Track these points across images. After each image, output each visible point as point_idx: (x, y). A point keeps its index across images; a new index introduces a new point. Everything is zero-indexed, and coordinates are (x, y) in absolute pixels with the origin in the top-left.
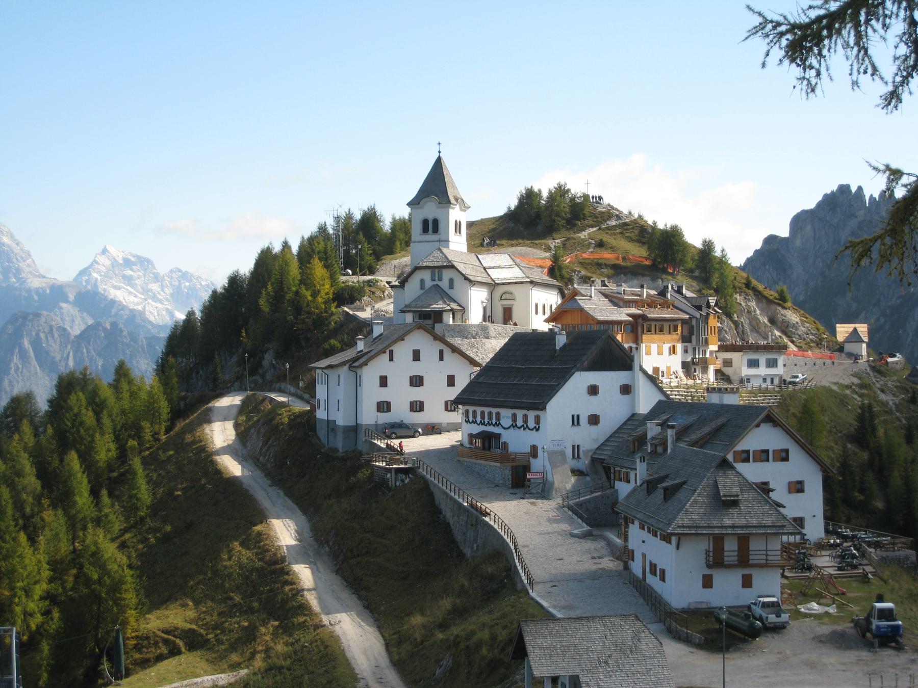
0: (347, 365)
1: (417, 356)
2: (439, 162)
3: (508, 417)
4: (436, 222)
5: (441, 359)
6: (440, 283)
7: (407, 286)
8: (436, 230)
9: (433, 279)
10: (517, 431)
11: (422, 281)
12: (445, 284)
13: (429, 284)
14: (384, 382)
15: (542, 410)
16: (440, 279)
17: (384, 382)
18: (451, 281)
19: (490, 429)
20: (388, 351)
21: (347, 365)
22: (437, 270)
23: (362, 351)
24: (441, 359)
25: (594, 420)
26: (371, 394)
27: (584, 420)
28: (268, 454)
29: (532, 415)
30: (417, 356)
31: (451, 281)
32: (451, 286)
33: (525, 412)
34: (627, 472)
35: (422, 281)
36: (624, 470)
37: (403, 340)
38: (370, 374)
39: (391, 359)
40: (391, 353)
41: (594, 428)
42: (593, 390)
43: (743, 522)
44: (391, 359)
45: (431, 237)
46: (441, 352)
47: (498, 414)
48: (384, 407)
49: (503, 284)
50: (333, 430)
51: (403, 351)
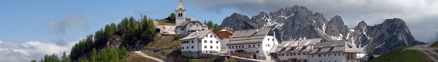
4: (182, 14)
8: (182, 16)
10: (250, 48)
11: (191, 25)
17: (206, 42)
19: (239, 49)
22: (194, 22)
27: (267, 45)
28: (171, 59)
31: (197, 25)
32: (197, 26)
33: (254, 44)
35: (191, 25)
43: (354, 50)
45: (180, 17)
48: (206, 47)
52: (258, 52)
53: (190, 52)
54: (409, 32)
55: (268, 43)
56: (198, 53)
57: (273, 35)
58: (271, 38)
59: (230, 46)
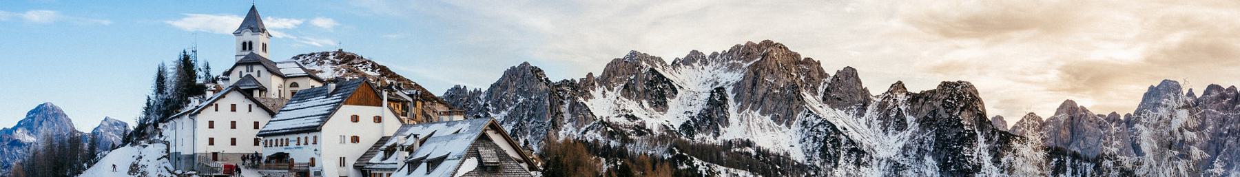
0: (188, 115)
1: (233, 108)
2: (253, 8)
3: (294, 141)
4: (251, 43)
5: (250, 111)
6: (251, 74)
7: (230, 77)
9: (247, 71)
11: (241, 72)
12: (254, 74)
13: (244, 74)
14: (211, 125)
15: (318, 131)
16: (252, 71)
17: (211, 125)
18: (259, 72)
20: (214, 104)
21: (188, 115)
23: (197, 107)
24: (250, 111)
25: (355, 139)
26: (203, 133)
27: (348, 139)
29: (311, 136)
30: (233, 108)
31: (259, 72)
32: (259, 76)
33: (306, 135)
34: (381, 174)
35: (241, 72)
36: (377, 172)
37: (224, 97)
38: (202, 120)
39: (217, 110)
40: (217, 105)
41: (356, 145)
42: (355, 119)
44: (217, 110)
46: (250, 106)
47: (287, 139)
49: (292, 77)
50: (179, 159)
51: (224, 104)
52: (313, 161)
53: (178, 156)
54: (81, 133)
55: (355, 129)
56: (191, 160)
57: (379, 103)
58: (367, 112)
59: (266, 138)
